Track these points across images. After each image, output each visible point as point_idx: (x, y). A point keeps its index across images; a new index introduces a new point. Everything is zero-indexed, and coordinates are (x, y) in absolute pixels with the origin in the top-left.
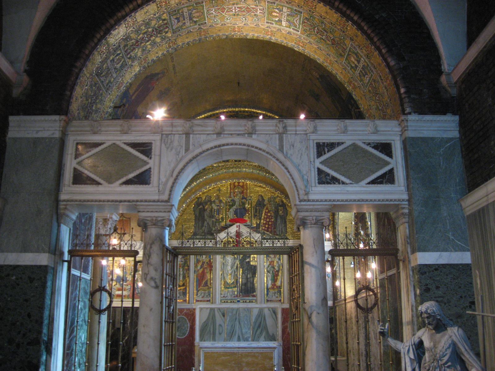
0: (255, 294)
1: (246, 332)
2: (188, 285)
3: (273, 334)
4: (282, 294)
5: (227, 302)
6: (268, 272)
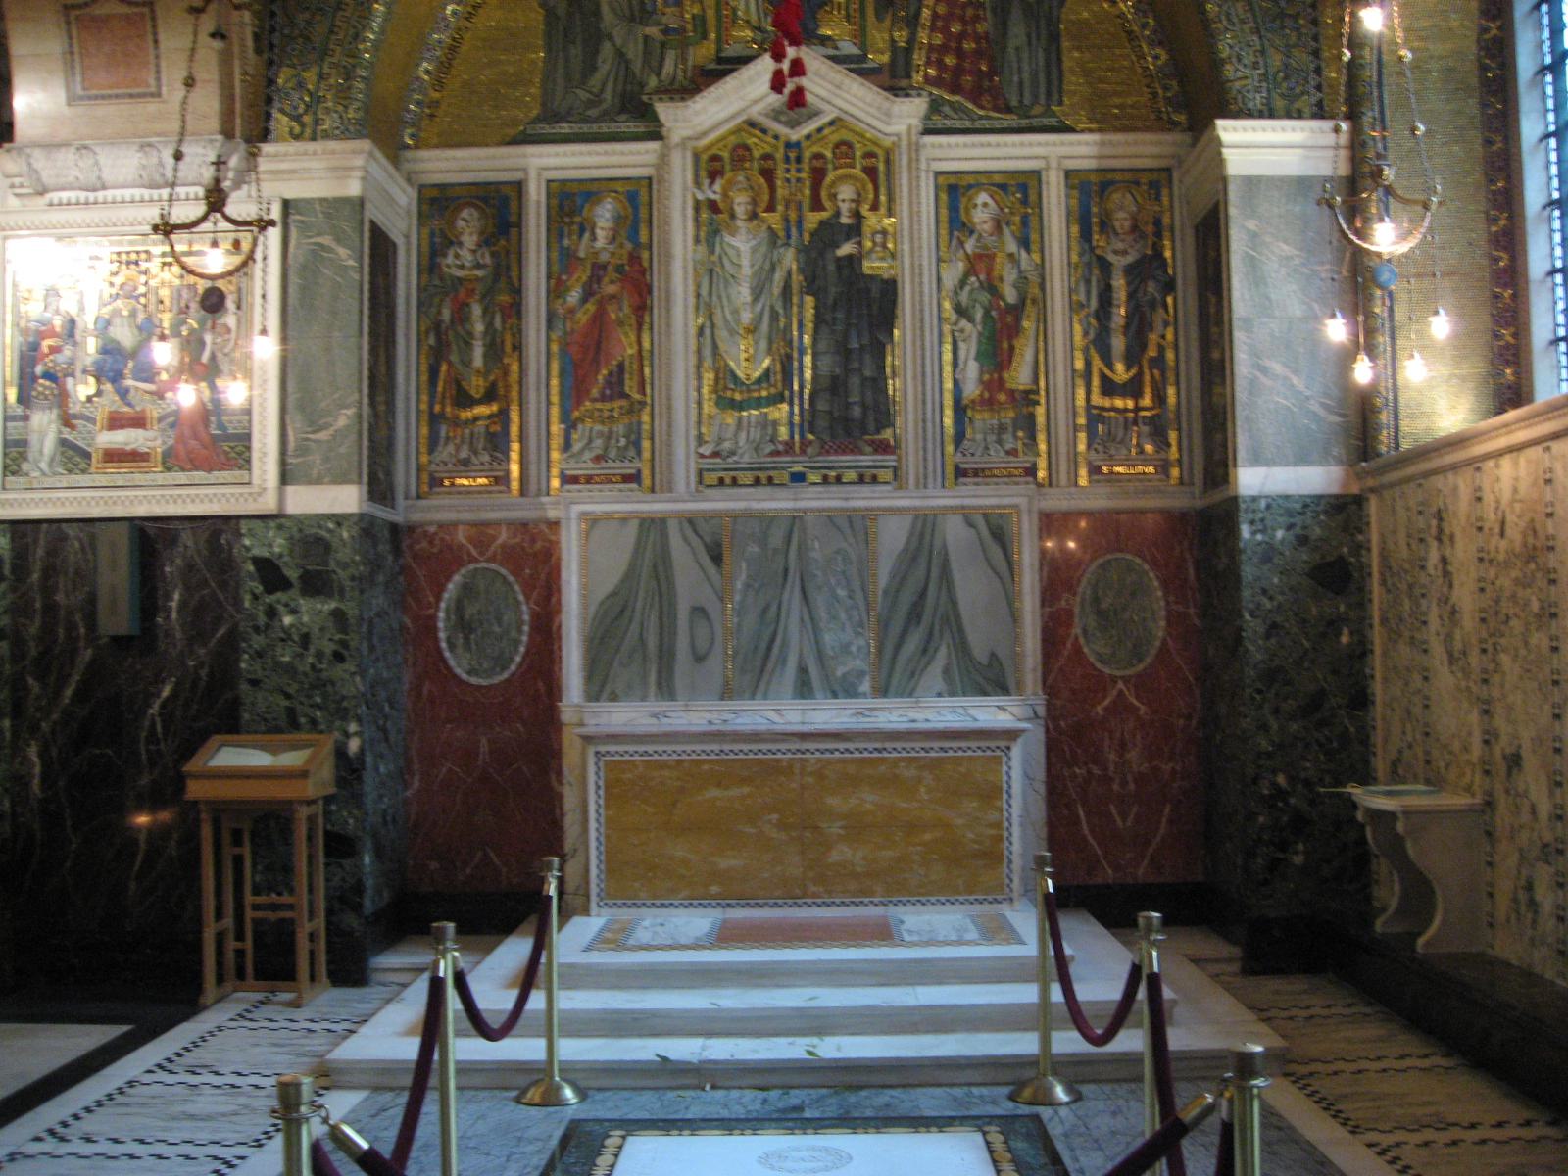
0: (887, 434)
1: (845, 648)
2: (514, 394)
3: (993, 655)
4: (1041, 437)
5: (735, 482)
6: (961, 311)
